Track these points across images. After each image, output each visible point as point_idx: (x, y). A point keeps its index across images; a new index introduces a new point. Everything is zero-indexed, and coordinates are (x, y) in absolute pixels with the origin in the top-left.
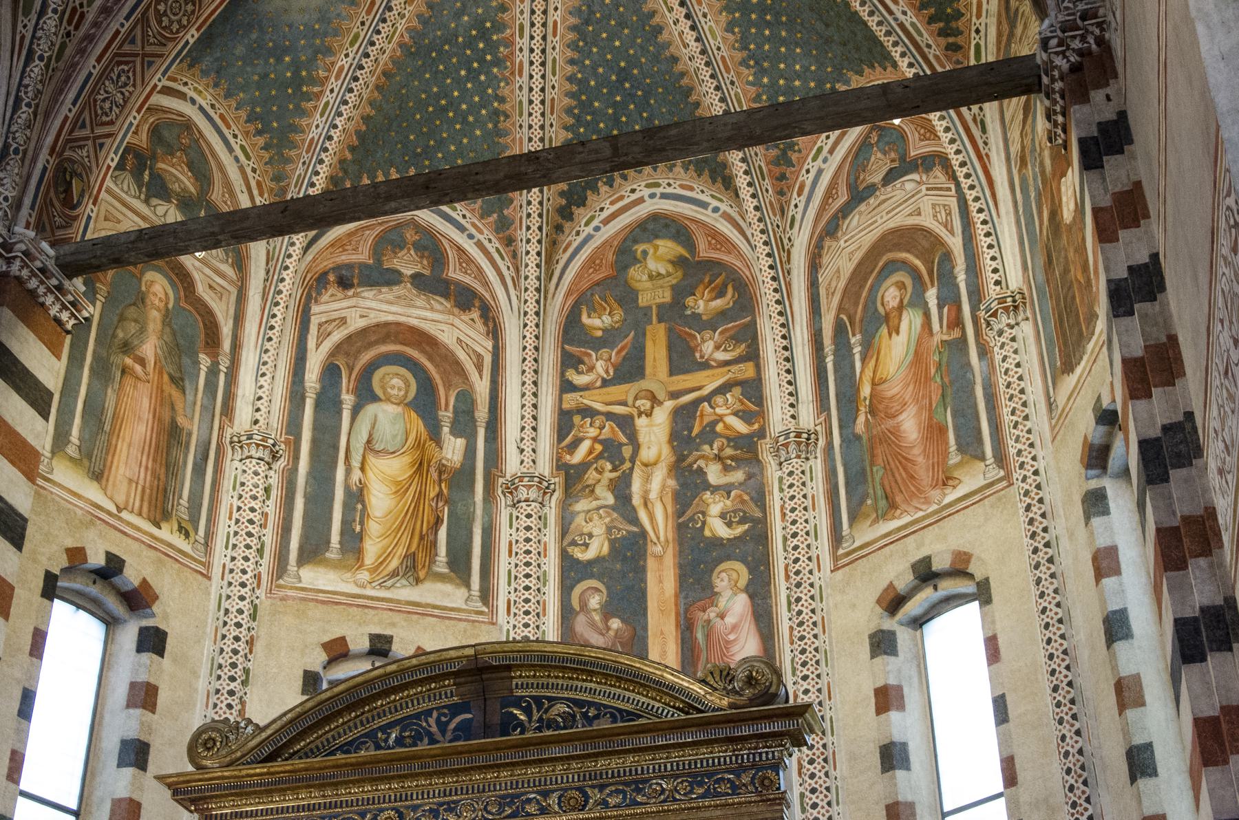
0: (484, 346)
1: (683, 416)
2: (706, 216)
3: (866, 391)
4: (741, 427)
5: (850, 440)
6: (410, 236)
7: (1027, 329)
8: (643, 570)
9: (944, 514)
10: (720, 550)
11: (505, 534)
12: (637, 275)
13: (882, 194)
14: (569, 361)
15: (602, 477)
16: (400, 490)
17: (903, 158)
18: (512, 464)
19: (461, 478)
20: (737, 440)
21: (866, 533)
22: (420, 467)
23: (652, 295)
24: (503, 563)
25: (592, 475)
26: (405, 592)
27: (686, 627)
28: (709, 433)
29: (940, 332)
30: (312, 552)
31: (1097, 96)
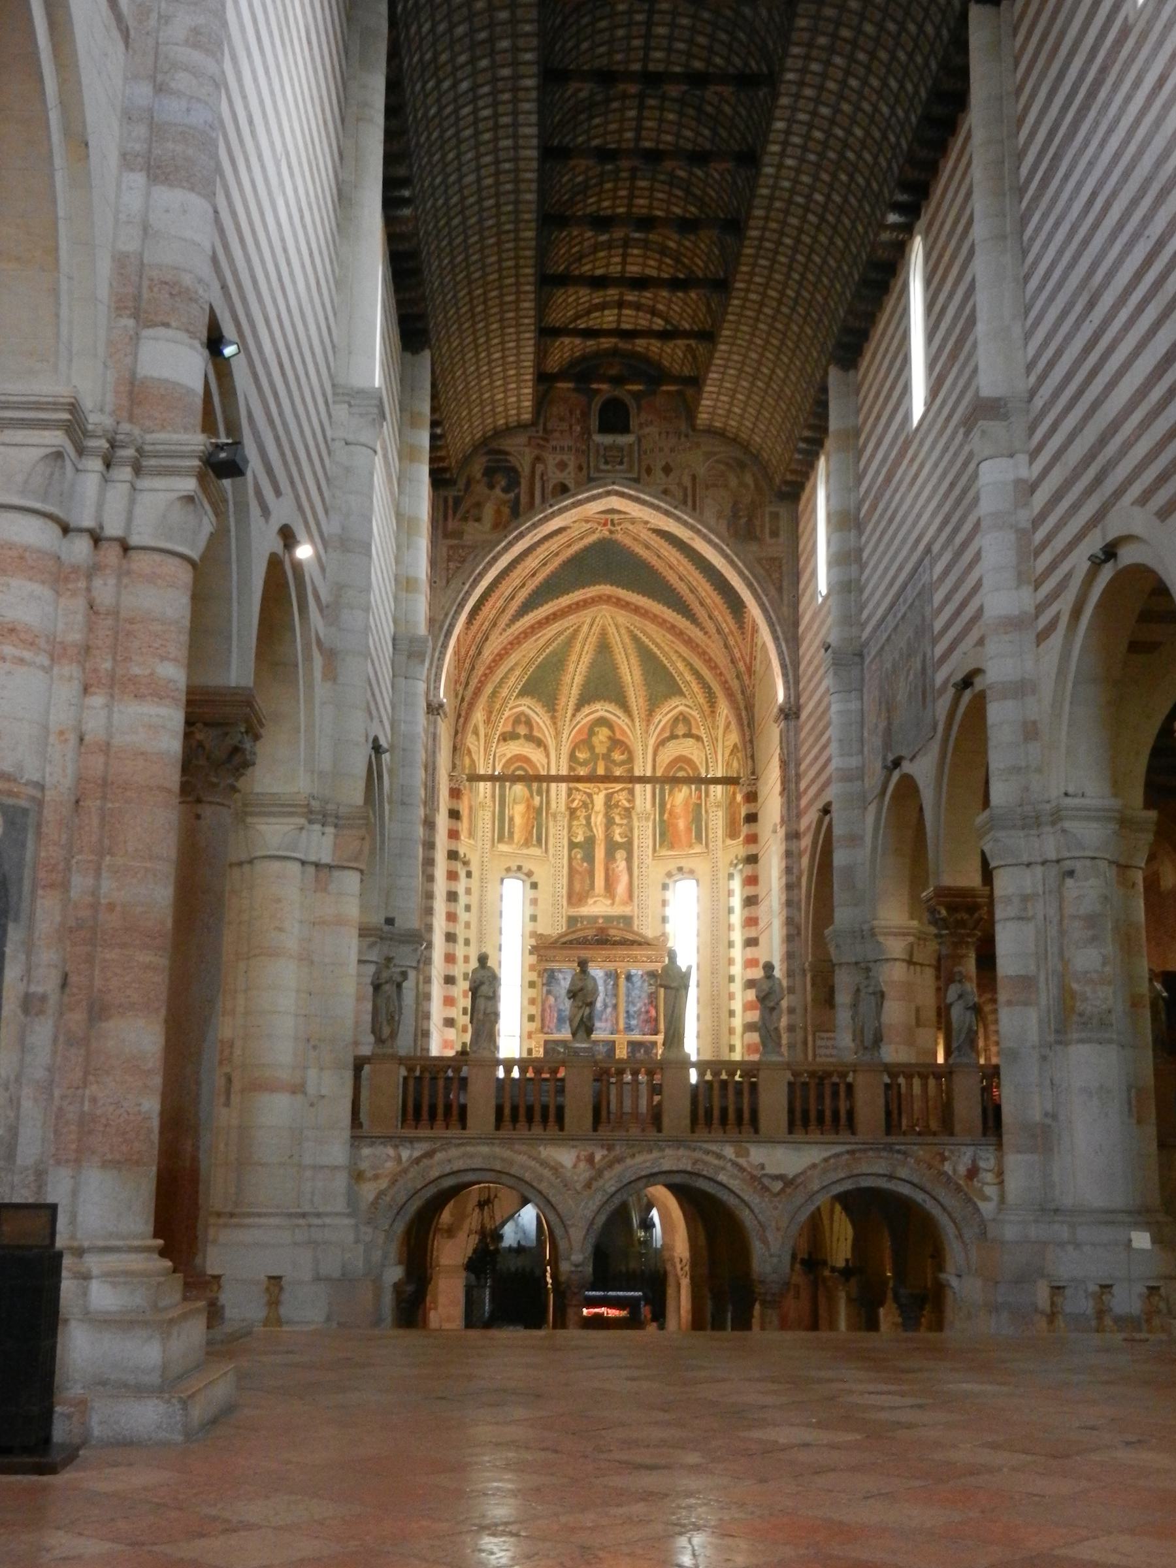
0: (545, 761)
1: (609, 797)
2: (620, 722)
3: (668, 806)
4: (627, 805)
5: (662, 821)
6: (523, 719)
7: (720, 813)
8: (593, 849)
9: (688, 856)
11: (552, 831)
12: (595, 740)
13: (682, 740)
15: (582, 814)
16: (523, 817)
17: (690, 730)
18: (553, 805)
19: (539, 811)
22: (528, 807)
23: (601, 749)
25: (578, 813)
26: (525, 851)
27: (607, 870)
28: (617, 805)
29: (694, 799)
30: (501, 839)
31: (753, 804)
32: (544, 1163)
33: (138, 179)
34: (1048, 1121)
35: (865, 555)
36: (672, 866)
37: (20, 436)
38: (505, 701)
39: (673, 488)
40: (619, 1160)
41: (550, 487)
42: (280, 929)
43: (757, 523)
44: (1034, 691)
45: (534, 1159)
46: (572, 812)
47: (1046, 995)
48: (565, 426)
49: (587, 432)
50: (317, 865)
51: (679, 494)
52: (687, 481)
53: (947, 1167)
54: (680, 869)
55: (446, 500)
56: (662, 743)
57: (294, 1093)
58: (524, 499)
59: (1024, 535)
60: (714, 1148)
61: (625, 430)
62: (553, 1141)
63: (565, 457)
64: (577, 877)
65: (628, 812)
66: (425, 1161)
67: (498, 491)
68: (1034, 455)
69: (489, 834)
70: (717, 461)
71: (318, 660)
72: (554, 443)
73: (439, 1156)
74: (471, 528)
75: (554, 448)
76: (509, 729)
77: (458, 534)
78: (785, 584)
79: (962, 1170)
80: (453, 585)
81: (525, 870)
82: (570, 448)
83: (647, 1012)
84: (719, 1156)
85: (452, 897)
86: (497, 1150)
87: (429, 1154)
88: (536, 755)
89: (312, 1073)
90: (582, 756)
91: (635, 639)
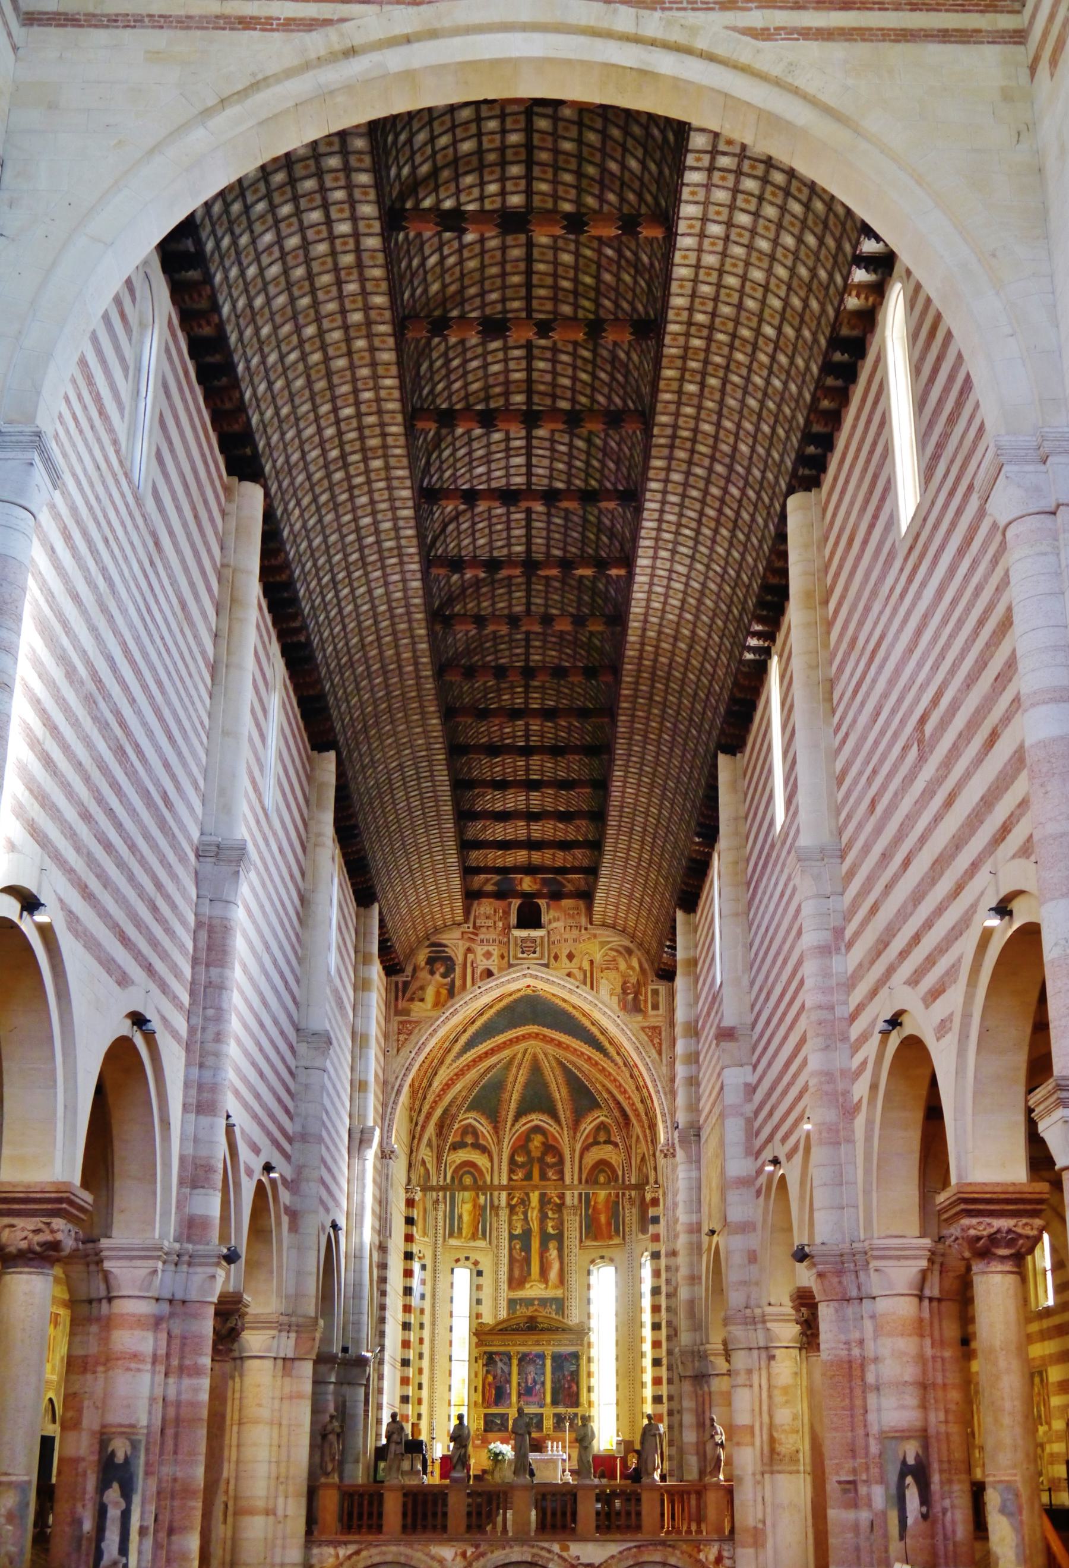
0: (489, 1165)
1: (543, 1196)
4: (558, 1201)
7: (634, 1210)
9: (609, 1246)
10: (550, 1237)
11: (495, 1225)
14: (511, 1171)
15: (520, 1209)
20: (556, 1205)
21: (589, 1243)
22: (474, 1206)
23: (536, 1154)
24: (494, 1234)
26: (472, 1244)
28: (549, 1202)
29: (613, 1198)
30: (451, 1235)
32: (433, 1558)
33: (192, 1116)
34: (760, 1526)
35: (701, 1058)
36: (594, 1254)
37: (139, 1263)
38: (454, 1117)
39: (576, 971)
40: (483, 1555)
41: (478, 971)
42: (259, 1405)
43: (642, 998)
44: (754, 1229)
45: (428, 1555)
46: (512, 1209)
47: (760, 1439)
48: (490, 923)
49: (507, 928)
50: (284, 1359)
51: (580, 976)
52: (586, 966)
53: (702, 1556)
54: (602, 1257)
55: (397, 983)
56: (586, 1149)
57: (267, 1514)
58: (458, 983)
59: (749, 1122)
60: (546, 1545)
61: (537, 924)
62: (442, 1542)
63: (490, 948)
64: (517, 1265)
65: (560, 1207)
66: (355, 1558)
67: (437, 977)
68: (755, 1067)
69: (441, 1231)
70: (611, 949)
71: (285, 1220)
72: (482, 937)
73: (364, 1554)
74: (416, 1006)
75: (482, 941)
76: (458, 1139)
77: (406, 1012)
78: (664, 1047)
79: (712, 1557)
80: (402, 1053)
81: (472, 1260)
82: (494, 941)
83: (570, 1387)
84: (549, 1551)
85: (408, 1291)
86: (402, 1549)
87: (357, 1553)
88: (481, 1161)
89: (281, 1501)
90: (520, 1159)
91: (560, 1063)
